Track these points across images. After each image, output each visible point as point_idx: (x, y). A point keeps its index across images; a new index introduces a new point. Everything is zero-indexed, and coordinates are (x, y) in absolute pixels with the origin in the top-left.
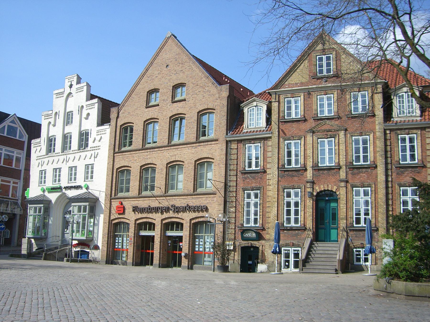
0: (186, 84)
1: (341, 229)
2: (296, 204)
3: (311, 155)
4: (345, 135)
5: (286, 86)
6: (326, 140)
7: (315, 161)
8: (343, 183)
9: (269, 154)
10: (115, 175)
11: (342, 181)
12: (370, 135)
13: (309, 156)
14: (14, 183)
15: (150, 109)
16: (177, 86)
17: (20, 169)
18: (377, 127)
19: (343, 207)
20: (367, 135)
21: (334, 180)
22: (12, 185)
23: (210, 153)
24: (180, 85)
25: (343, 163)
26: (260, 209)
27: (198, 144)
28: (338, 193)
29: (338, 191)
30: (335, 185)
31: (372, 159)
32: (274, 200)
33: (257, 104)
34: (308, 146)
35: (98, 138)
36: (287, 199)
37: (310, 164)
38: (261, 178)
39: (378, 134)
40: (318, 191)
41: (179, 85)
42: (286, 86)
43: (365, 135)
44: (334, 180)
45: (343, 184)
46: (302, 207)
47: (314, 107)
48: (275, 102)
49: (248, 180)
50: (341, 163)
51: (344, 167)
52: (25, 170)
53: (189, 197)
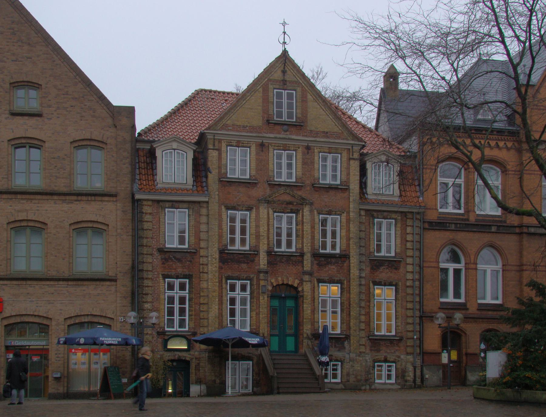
0: (41, 85)
2: (182, 300)
3: (265, 234)
4: (311, 211)
5: (230, 128)
6: (285, 216)
8: (307, 276)
9: (203, 227)
11: (305, 273)
12: (341, 214)
13: (262, 236)
16: (20, 84)
18: (351, 206)
20: (338, 215)
23: (100, 215)
24: (26, 84)
25: (307, 249)
26: (189, 307)
27: (75, 198)
28: (300, 289)
30: (297, 279)
31: (344, 247)
32: (214, 294)
33: (178, 146)
34: (261, 221)
36: (230, 294)
37: (263, 248)
38: (191, 261)
41: (23, 84)
42: (230, 128)
45: (306, 278)
46: (253, 306)
47: (271, 166)
48: (213, 149)
49: (171, 263)
50: (305, 250)
51: (309, 255)
53: (61, 283)
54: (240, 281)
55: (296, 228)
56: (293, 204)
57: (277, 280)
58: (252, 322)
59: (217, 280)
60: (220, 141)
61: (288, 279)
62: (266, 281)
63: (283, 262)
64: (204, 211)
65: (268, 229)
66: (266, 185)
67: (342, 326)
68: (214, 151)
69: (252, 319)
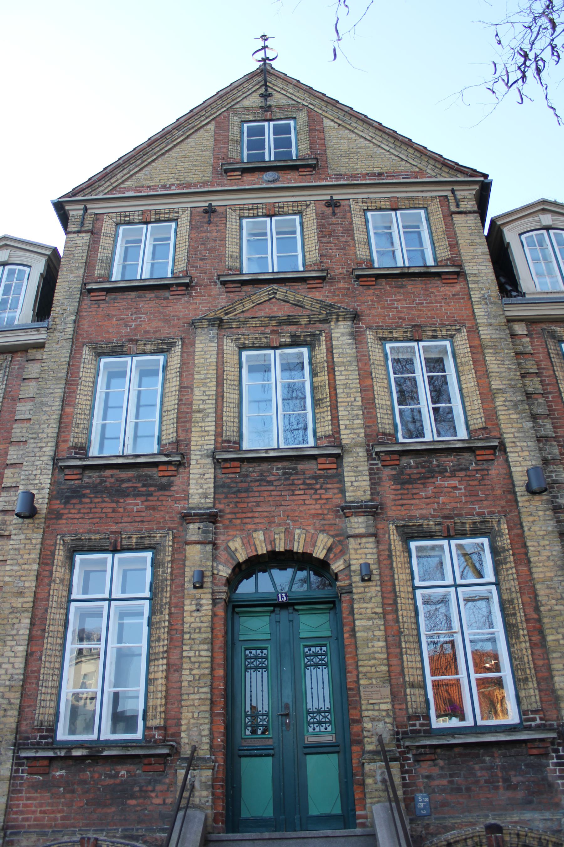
1: (369, 748)
3: (210, 406)
4: (356, 335)
7: (229, 432)
8: (361, 519)
12: (452, 337)
13: (200, 411)
18: (480, 311)
19: (367, 629)
20: (444, 338)
21: (315, 508)
28: (337, 566)
29: (337, 558)
30: (323, 531)
31: (478, 421)
32: (18, 602)
34: (198, 373)
39: (485, 333)
40: (242, 557)
43: (435, 337)
44: (315, 508)
46: (158, 640)
47: (231, 249)
50: (346, 438)
51: (361, 452)
54: (117, 556)
55: (312, 383)
56: (297, 323)
57: (248, 541)
58: (151, 703)
59: (35, 556)
60: (98, 217)
61: (289, 533)
62: (209, 548)
63: (270, 483)
64: (33, 370)
65: (220, 396)
66: (218, 289)
67: (522, 694)
68: (80, 235)
69: (151, 688)
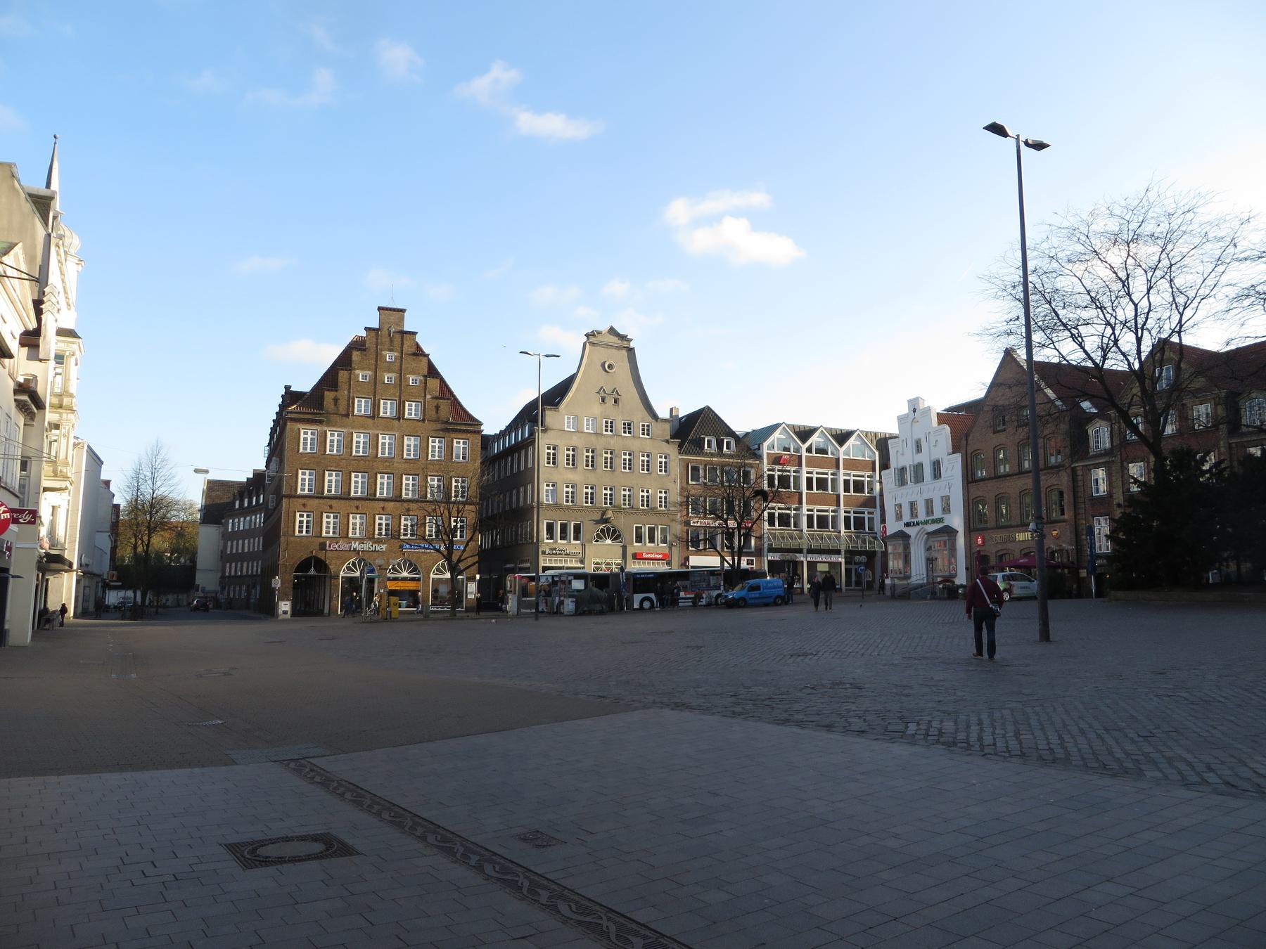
10: (971, 507)
14: (869, 513)
15: (997, 434)
17: (874, 495)
22: (866, 516)
35: (950, 467)
39: (1222, 449)
52: (880, 495)
